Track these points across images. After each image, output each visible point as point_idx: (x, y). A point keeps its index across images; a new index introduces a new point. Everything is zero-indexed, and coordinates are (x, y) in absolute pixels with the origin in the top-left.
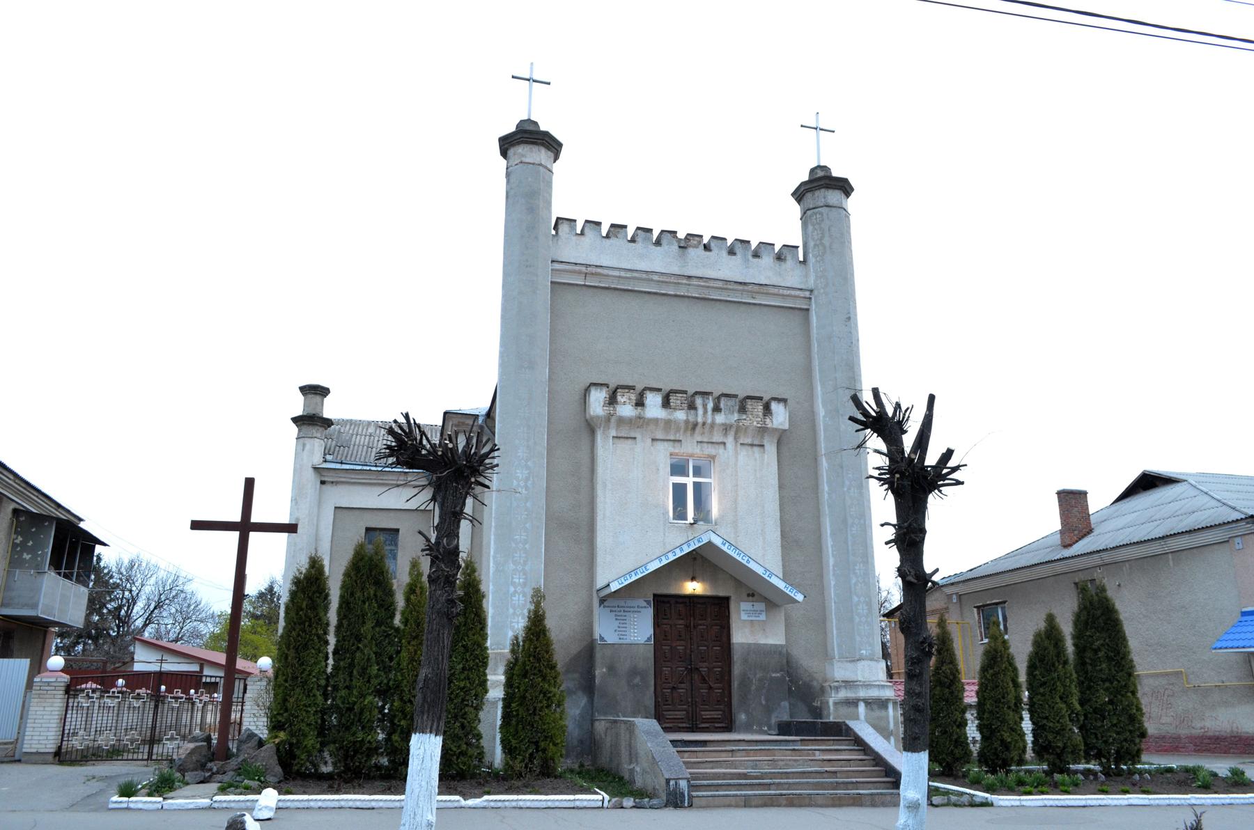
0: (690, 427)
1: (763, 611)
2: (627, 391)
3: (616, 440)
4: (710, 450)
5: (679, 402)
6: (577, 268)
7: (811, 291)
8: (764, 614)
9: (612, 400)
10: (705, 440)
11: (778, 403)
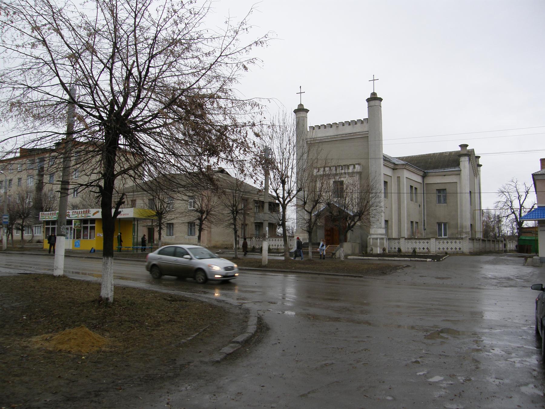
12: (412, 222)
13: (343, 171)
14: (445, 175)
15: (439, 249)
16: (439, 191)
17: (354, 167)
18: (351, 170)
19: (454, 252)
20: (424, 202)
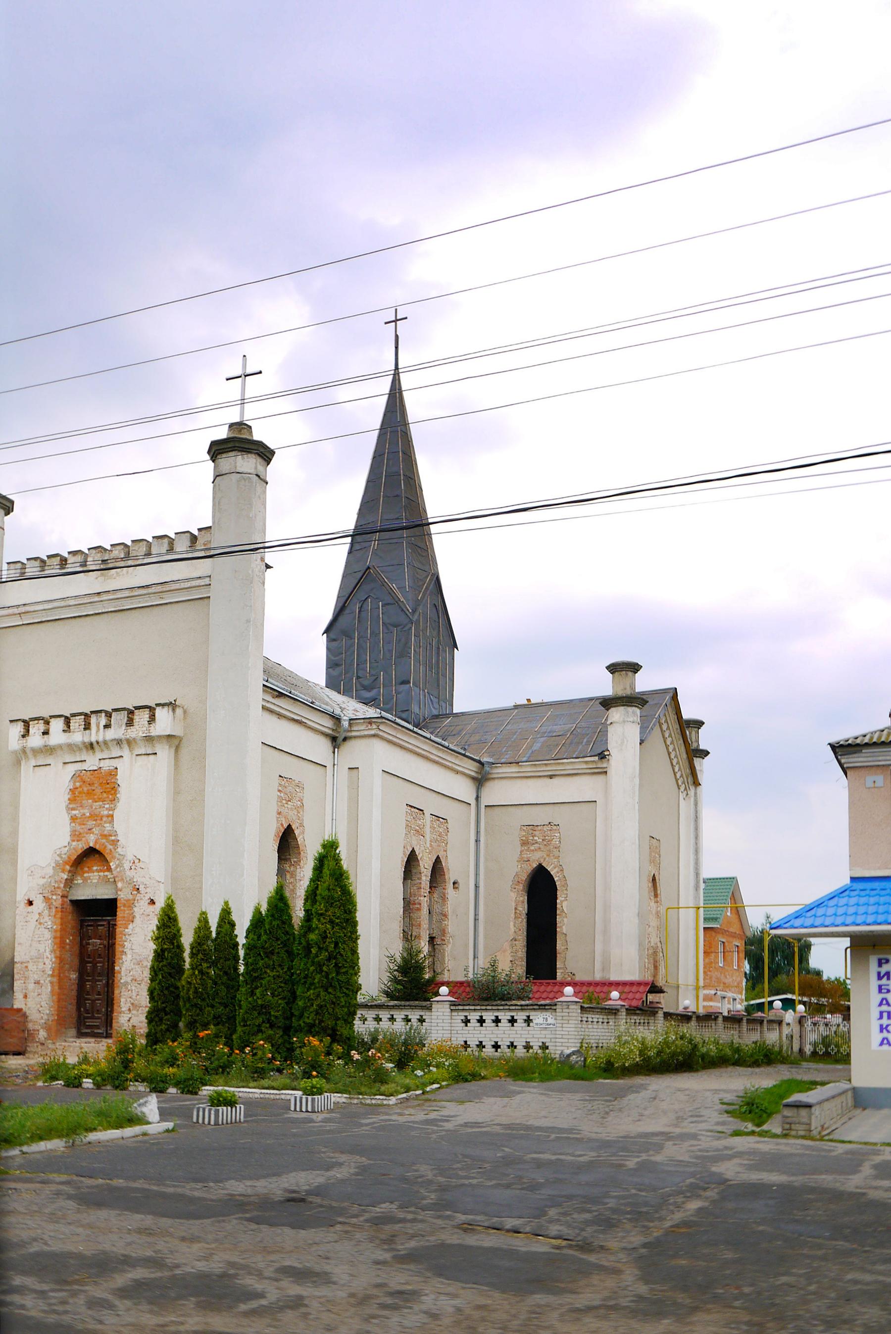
0: (89, 746)
2: (36, 722)
4: (114, 763)
5: (77, 724)
6: (10, 611)
9: (26, 734)
13: (111, 734)
14: (551, 777)
17: (152, 719)
19: (522, 1059)
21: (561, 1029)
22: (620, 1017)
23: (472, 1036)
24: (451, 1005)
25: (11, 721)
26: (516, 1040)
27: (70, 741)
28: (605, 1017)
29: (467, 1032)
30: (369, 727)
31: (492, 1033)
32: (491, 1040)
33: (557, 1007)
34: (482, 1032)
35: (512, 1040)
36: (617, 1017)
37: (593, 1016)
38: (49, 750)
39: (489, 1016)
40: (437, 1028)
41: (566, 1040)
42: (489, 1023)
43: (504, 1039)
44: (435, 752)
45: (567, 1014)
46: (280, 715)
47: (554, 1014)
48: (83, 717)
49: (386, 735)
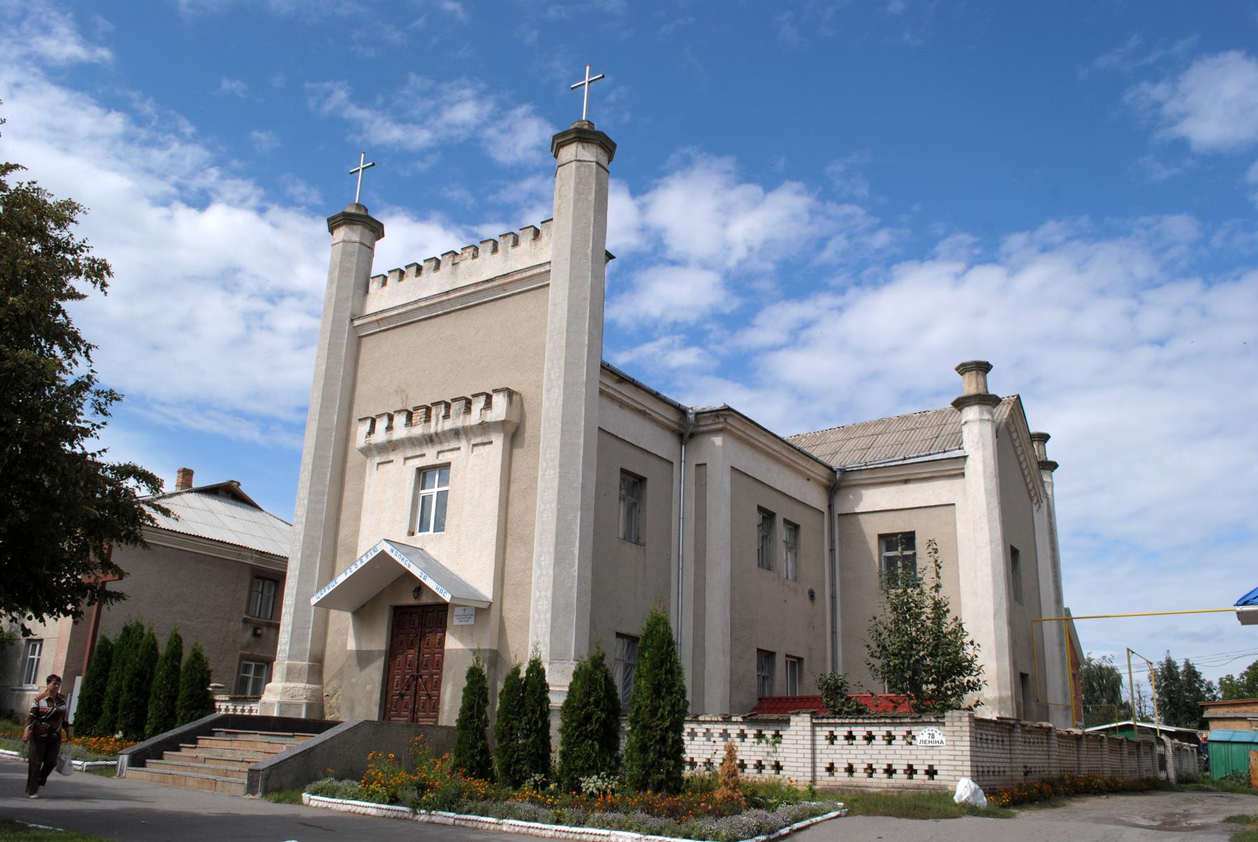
1: (471, 615)
3: (380, 466)
5: (419, 418)
7: (550, 262)
8: (473, 617)
10: (446, 448)
11: (634, 380)
12: (766, 657)
13: (449, 425)
14: (906, 482)
15: (831, 769)
16: (887, 540)
17: (488, 404)
18: (474, 418)
19: (904, 787)
20: (833, 585)
21: (952, 748)
22: (1016, 735)
23: (839, 756)
24: (812, 718)
25: (360, 420)
26: (895, 762)
27: (409, 435)
28: (1000, 734)
29: (833, 752)
30: (717, 421)
31: (865, 754)
32: (863, 763)
33: (946, 719)
34: (852, 752)
35: (890, 762)
36: (1012, 734)
37: (987, 733)
38: (391, 446)
39: (860, 732)
40: (797, 746)
41: (960, 763)
42: (859, 740)
43: (880, 761)
44: (785, 453)
45: (959, 729)
46: (622, 404)
47: (942, 728)
48: (424, 410)
49: (734, 430)
